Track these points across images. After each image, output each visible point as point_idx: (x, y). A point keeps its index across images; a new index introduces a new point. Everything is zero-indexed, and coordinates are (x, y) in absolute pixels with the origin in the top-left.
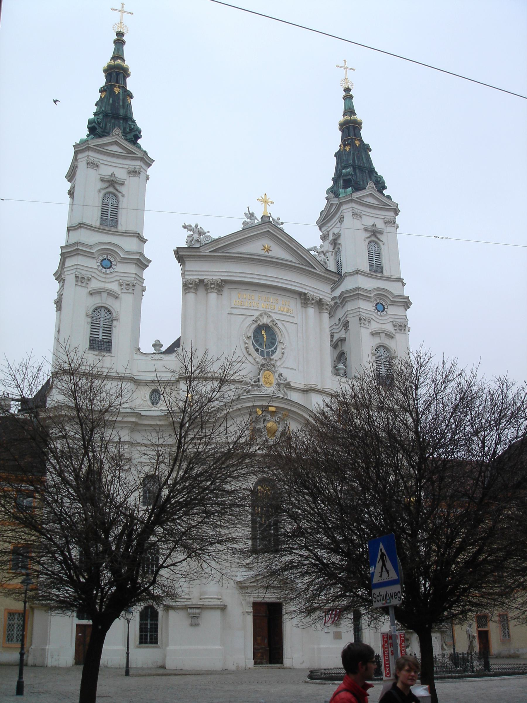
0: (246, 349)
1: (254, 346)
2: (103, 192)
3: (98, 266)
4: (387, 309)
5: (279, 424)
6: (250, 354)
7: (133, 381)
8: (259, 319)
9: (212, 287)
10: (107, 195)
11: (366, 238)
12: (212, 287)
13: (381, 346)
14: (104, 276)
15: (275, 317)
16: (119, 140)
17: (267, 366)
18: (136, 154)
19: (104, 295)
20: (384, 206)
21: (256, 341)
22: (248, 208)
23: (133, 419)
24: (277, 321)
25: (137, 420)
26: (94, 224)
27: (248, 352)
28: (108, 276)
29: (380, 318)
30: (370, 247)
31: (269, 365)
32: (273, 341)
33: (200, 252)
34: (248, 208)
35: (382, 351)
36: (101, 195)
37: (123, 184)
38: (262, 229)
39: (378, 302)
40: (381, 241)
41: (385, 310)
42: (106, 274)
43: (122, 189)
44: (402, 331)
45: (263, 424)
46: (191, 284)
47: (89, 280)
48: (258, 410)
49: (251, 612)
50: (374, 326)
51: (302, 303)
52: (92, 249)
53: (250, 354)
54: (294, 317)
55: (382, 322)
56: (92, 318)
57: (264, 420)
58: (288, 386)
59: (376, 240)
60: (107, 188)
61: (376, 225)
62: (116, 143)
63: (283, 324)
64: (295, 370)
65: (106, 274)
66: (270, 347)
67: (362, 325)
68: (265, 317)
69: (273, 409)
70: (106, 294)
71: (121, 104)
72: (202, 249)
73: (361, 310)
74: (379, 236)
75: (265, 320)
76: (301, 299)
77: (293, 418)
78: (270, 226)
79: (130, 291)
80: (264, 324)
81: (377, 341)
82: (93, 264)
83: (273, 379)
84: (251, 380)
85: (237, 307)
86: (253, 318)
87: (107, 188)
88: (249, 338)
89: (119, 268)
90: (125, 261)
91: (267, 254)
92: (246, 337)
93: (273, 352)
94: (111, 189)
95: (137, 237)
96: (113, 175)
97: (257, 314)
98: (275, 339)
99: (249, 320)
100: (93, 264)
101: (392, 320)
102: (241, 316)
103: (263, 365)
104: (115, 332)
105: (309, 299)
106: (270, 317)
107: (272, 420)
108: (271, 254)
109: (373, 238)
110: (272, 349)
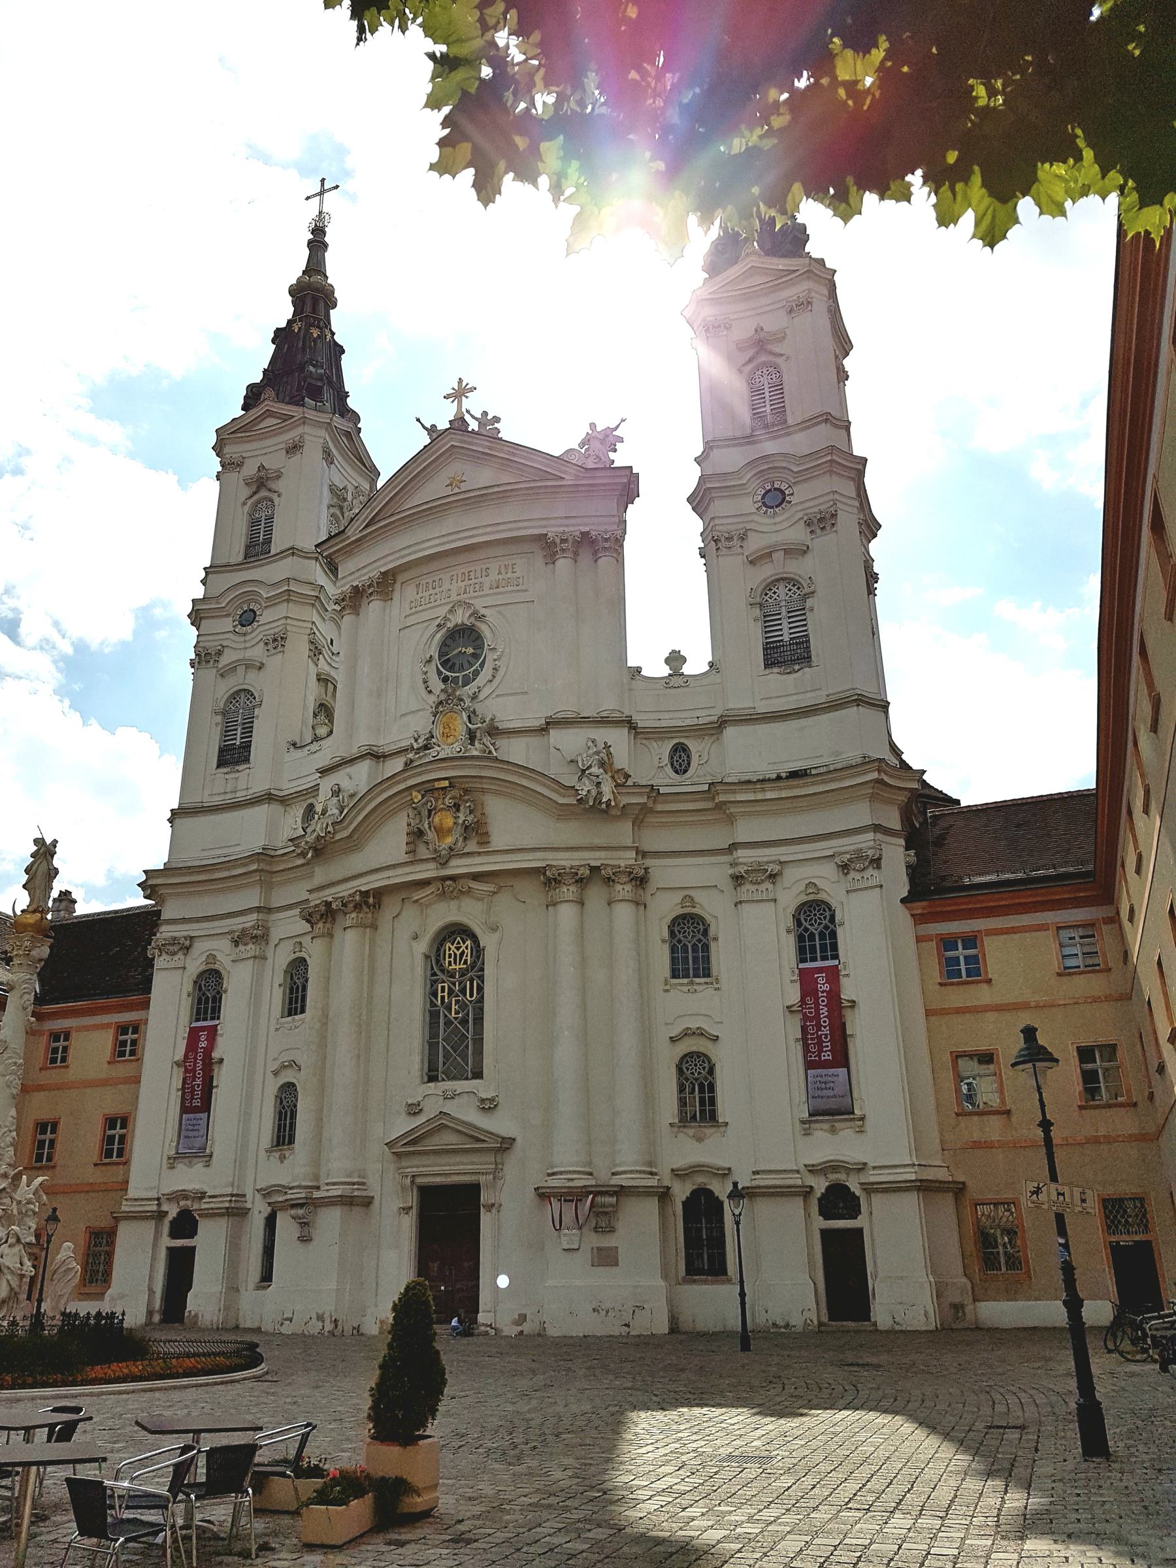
1: (439, 673)
2: (250, 502)
3: (234, 626)
4: (792, 494)
5: (458, 810)
6: (430, 692)
7: (276, 800)
8: (449, 620)
9: (371, 590)
10: (260, 506)
11: (744, 365)
12: (371, 590)
13: (778, 580)
14: (242, 639)
15: (478, 604)
16: (272, 406)
18: (293, 416)
19: (241, 670)
20: (782, 277)
21: (444, 664)
22: (418, 420)
23: (254, 867)
24: (483, 611)
25: (262, 866)
26: (233, 561)
28: (248, 638)
29: (772, 521)
30: (758, 380)
31: (450, 702)
32: (478, 652)
33: (348, 538)
34: (418, 420)
35: (782, 590)
36: (246, 508)
37: (278, 477)
38: (440, 448)
39: (768, 488)
40: (782, 355)
41: (787, 498)
42: (245, 635)
43: (279, 485)
44: (828, 528)
46: (343, 600)
47: (219, 653)
48: (414, 794)
49: (411, 1208)
50: (754, 544)
51: (545, 556)
52: (219, 603)
53: (430, 692)
54: (526, 591)
55: (778, 527)
56: (224, 713)
57: (430, 811)
58: (494, 731)
59: (771, 358)
60: (255, 493)
61: (762, 329)
62: (269, 414)
63: (500, 612)
64: (526, 693)
65: (245, 635)
66: (471, 665)
67: (724, 551)
68: (460, 611)
69: (446, 783)
70: (244, 667)
71: (300, 344)
72: (349, 532)
73: (717, 521)
74: (777, 349)
75: (461, 617)
76: (543, 549)
77: (497, 793)
78: (453, 436)
79: (280, 649)
80: (456, 625)
81: (767, 571)
82: (227, 624)
83: (460, 725)
84: (416, 740)
85: (414, 610)
86: (437, 622)
87: (255, 493)
88: (430, 661)
89: (265, 617)
90: (272, 602)
91: (456, 490)
93: (476, 673)
94: (263, 493)
95: (293, 554)
96: (262, 467)
97: (442, 611)
98: (481, 647)
99: (433, 627)
100: (227, 624)
101: (800, 515)
102: (420, 626)
104: (255, 725)
106: (469, 605)
107: (442, 806)
108: (464, 487)
109: (763, 358)
110: (474, 668)
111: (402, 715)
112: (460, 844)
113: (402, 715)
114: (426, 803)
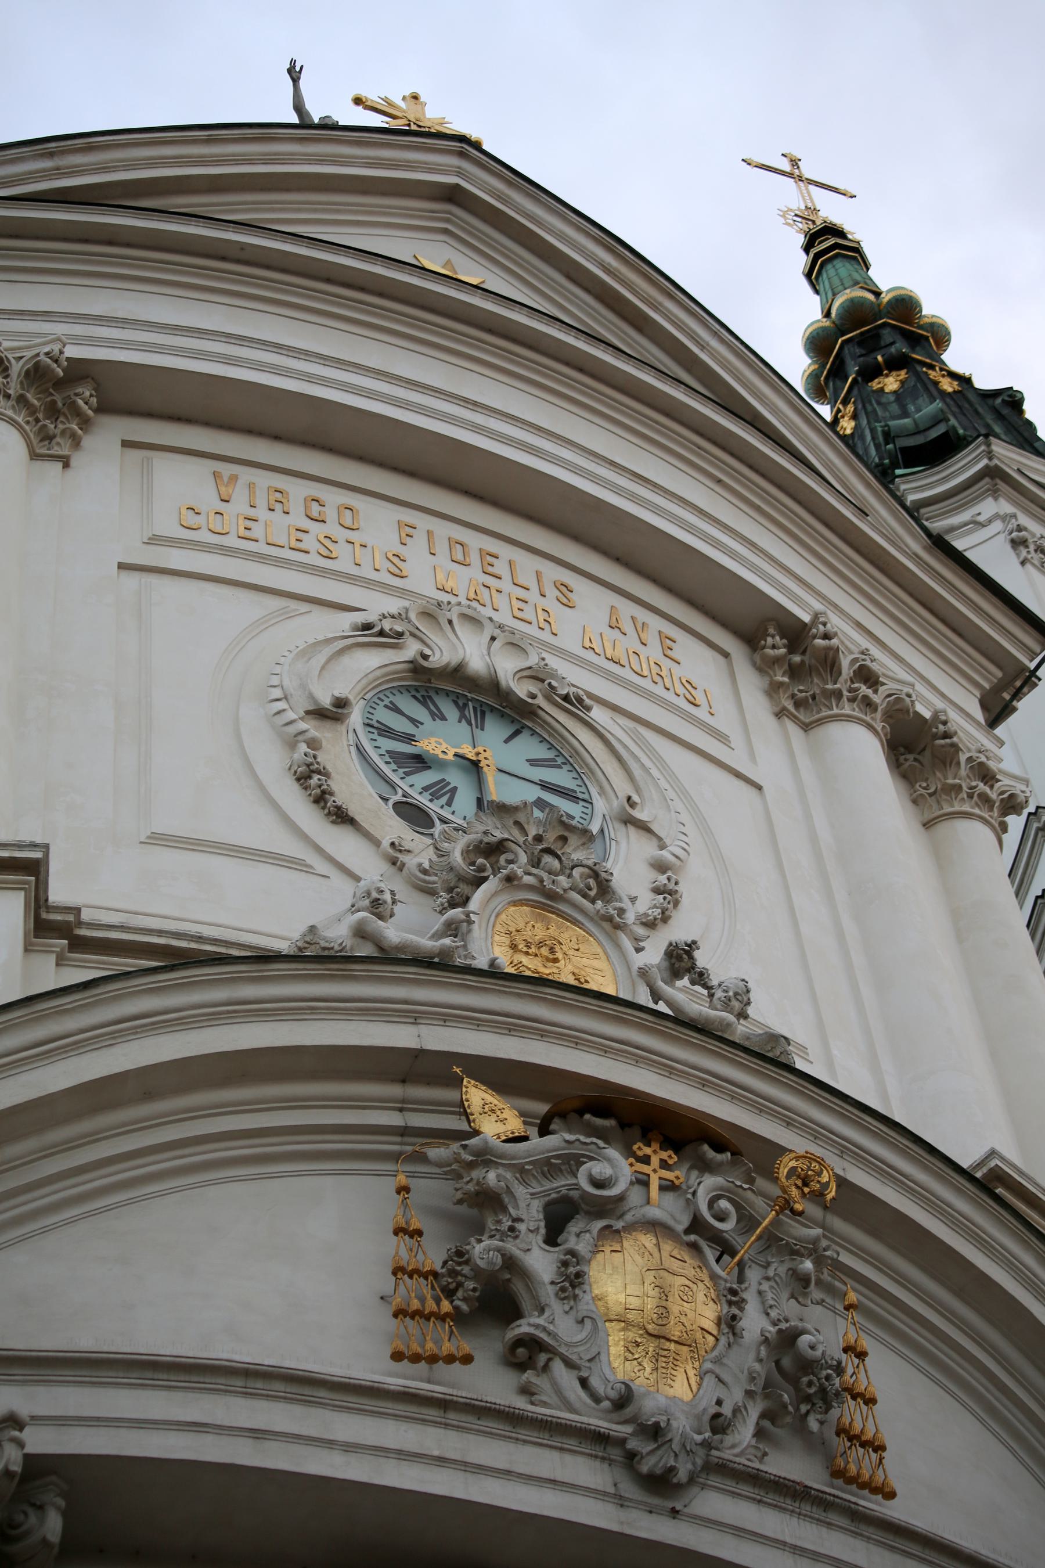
0: (302, 779)
6: (341, 817)
17: (536, 863)
27: (321, 799)
45: (551, 1240)
48: (476, 1095)
51: (773, 690)
53: (341, 817)
54: (722, 738)
76: (764, 667)
92: (303, 705)
103: (493, 850)
105: (829, 662)
111: (158, 840)
112: (744, 1433)
113: (158, 840)
114: (549, 1167)
